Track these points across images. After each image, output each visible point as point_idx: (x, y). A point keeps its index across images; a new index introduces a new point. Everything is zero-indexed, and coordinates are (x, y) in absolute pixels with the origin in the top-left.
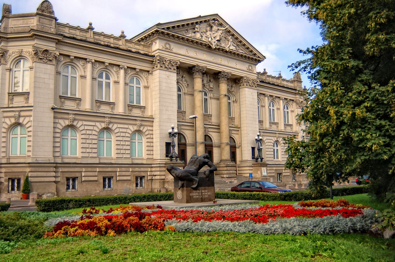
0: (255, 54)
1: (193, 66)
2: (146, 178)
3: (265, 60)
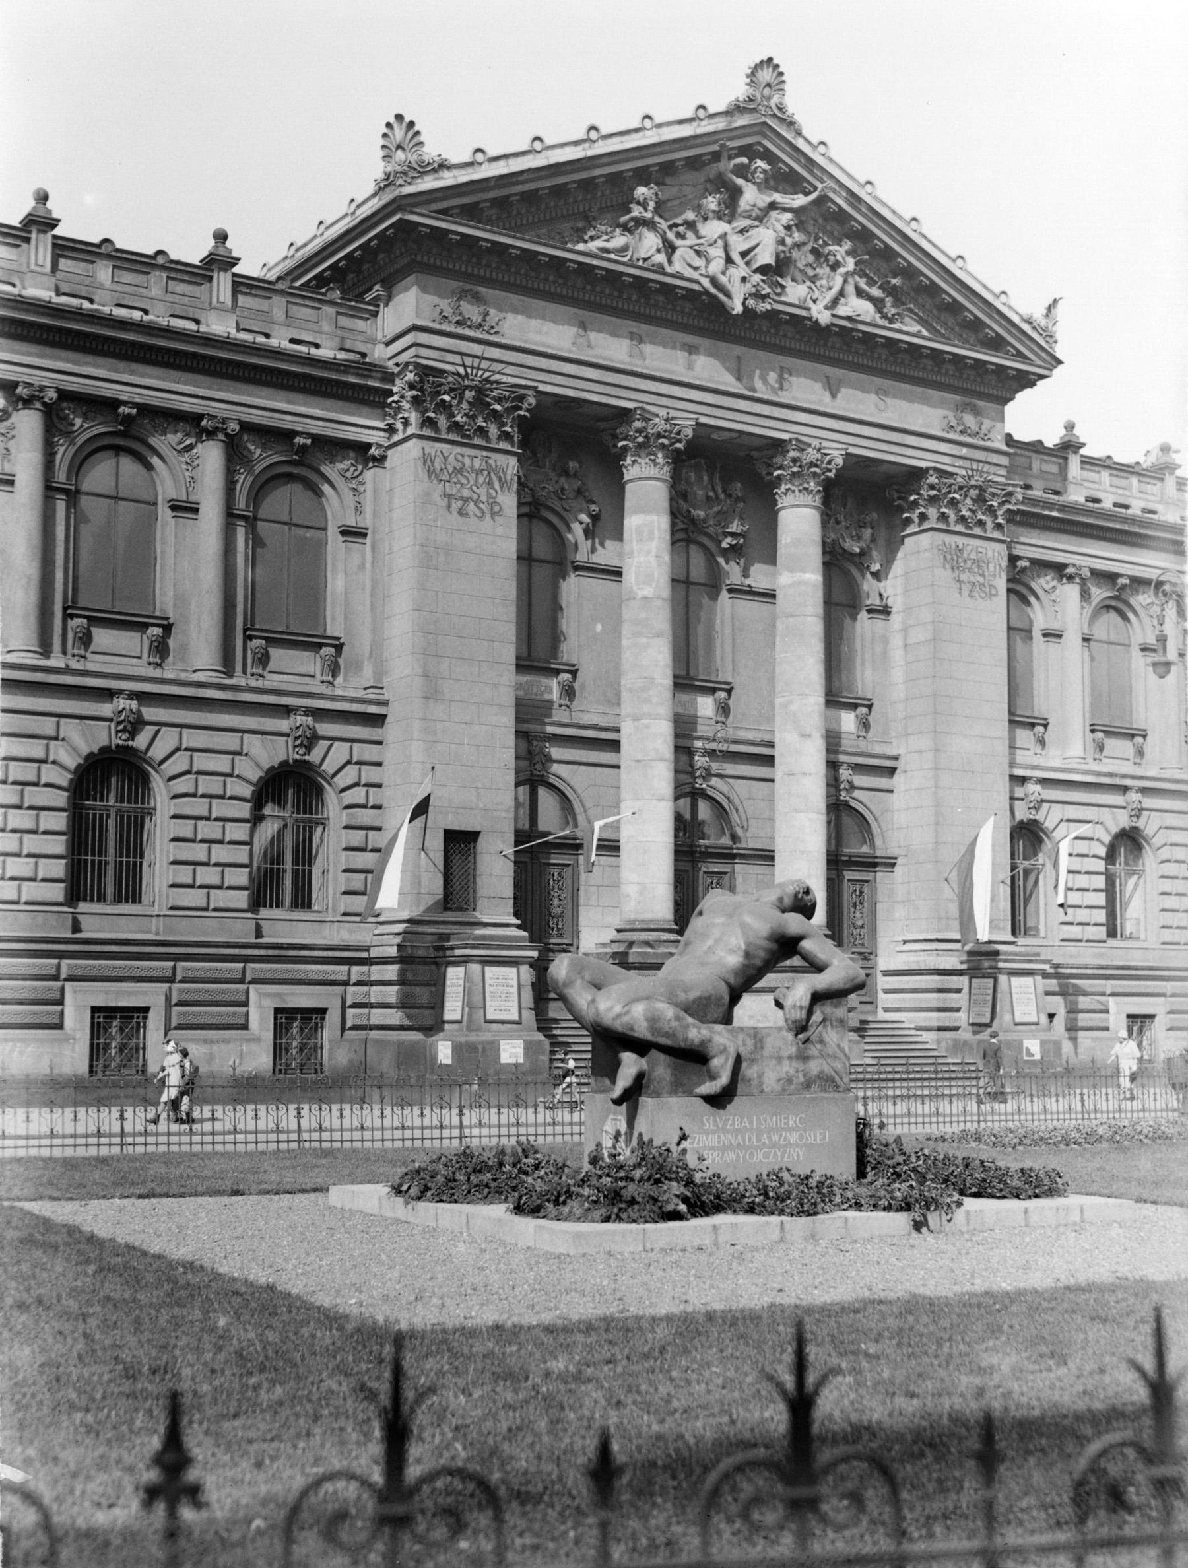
0: (997, 344)
2: (333, 1018)
3: (1058, 372)
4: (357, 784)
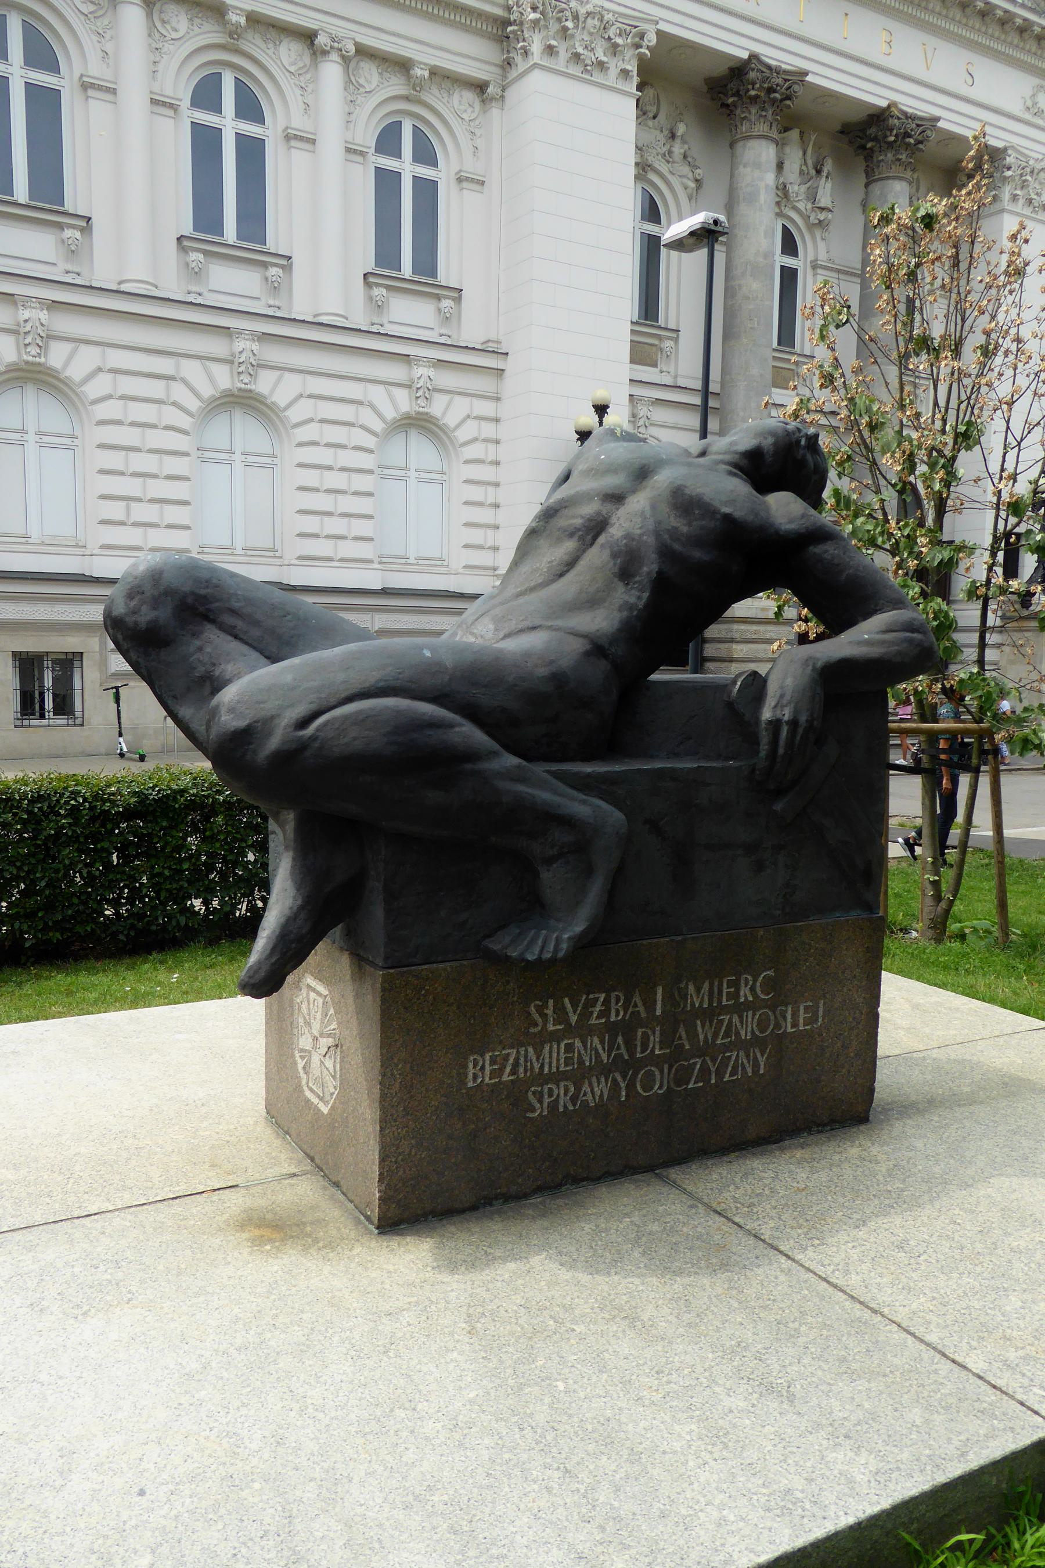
1: (732, 70)
4: (475, 440)
